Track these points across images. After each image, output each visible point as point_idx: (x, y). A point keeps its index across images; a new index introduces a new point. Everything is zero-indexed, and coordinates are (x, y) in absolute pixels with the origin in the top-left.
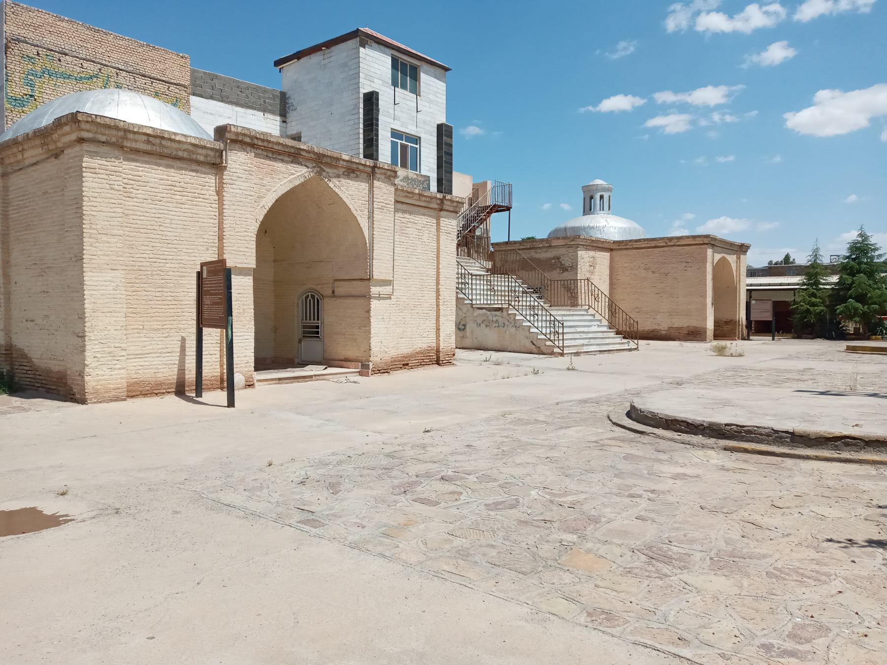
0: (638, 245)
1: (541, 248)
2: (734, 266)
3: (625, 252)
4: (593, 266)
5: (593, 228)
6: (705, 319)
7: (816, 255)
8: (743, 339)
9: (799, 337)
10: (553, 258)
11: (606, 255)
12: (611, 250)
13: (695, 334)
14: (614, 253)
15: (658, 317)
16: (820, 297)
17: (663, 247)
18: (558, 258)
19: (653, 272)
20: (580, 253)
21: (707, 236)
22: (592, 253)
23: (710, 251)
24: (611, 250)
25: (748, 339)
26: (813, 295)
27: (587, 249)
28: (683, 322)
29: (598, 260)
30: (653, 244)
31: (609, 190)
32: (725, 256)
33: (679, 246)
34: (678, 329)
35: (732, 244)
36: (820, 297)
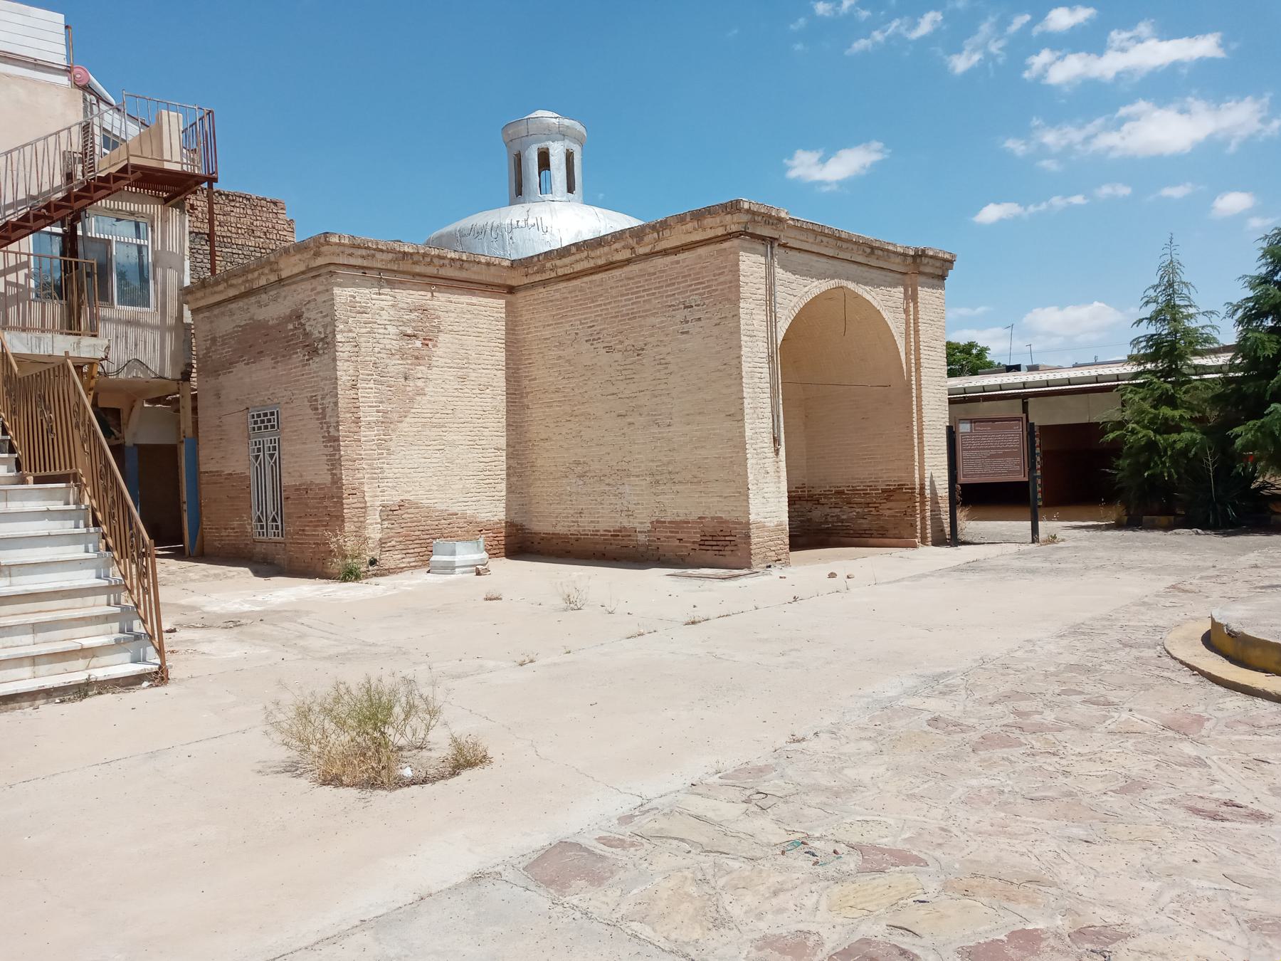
0: (564, 265)
1: (264, 289)
2: (895, 323)
3: (541, 293)
4: (420, 337)
5: (480, 232)
6: (743, 493)
7: (1171, 285)
8: (939, 541)
9: (1131, 522)
10: (289, 319)
11: (497, 305)
12: (511, 290)
13: (716, 546)
14: (520, 297)
15: (627, 489)
16: (1190, 408)
17: (628, 262)
18: (299, 317)
19: (609, 349)
20: (342, 294)
21: (734, 207)
22: (412, 297)
23: (751, 264)
24: (511, 290)
25: (955, 540)
26: (1171, 401)
27: (380, 283)
28: (689, 505)
29: (447, 320)
30: (601, 256)
31: (563, 134)
32: (851, 285)
33: (665, 253)
34: (678, 525)
35: (872, 249)
36: (1190, 408)
